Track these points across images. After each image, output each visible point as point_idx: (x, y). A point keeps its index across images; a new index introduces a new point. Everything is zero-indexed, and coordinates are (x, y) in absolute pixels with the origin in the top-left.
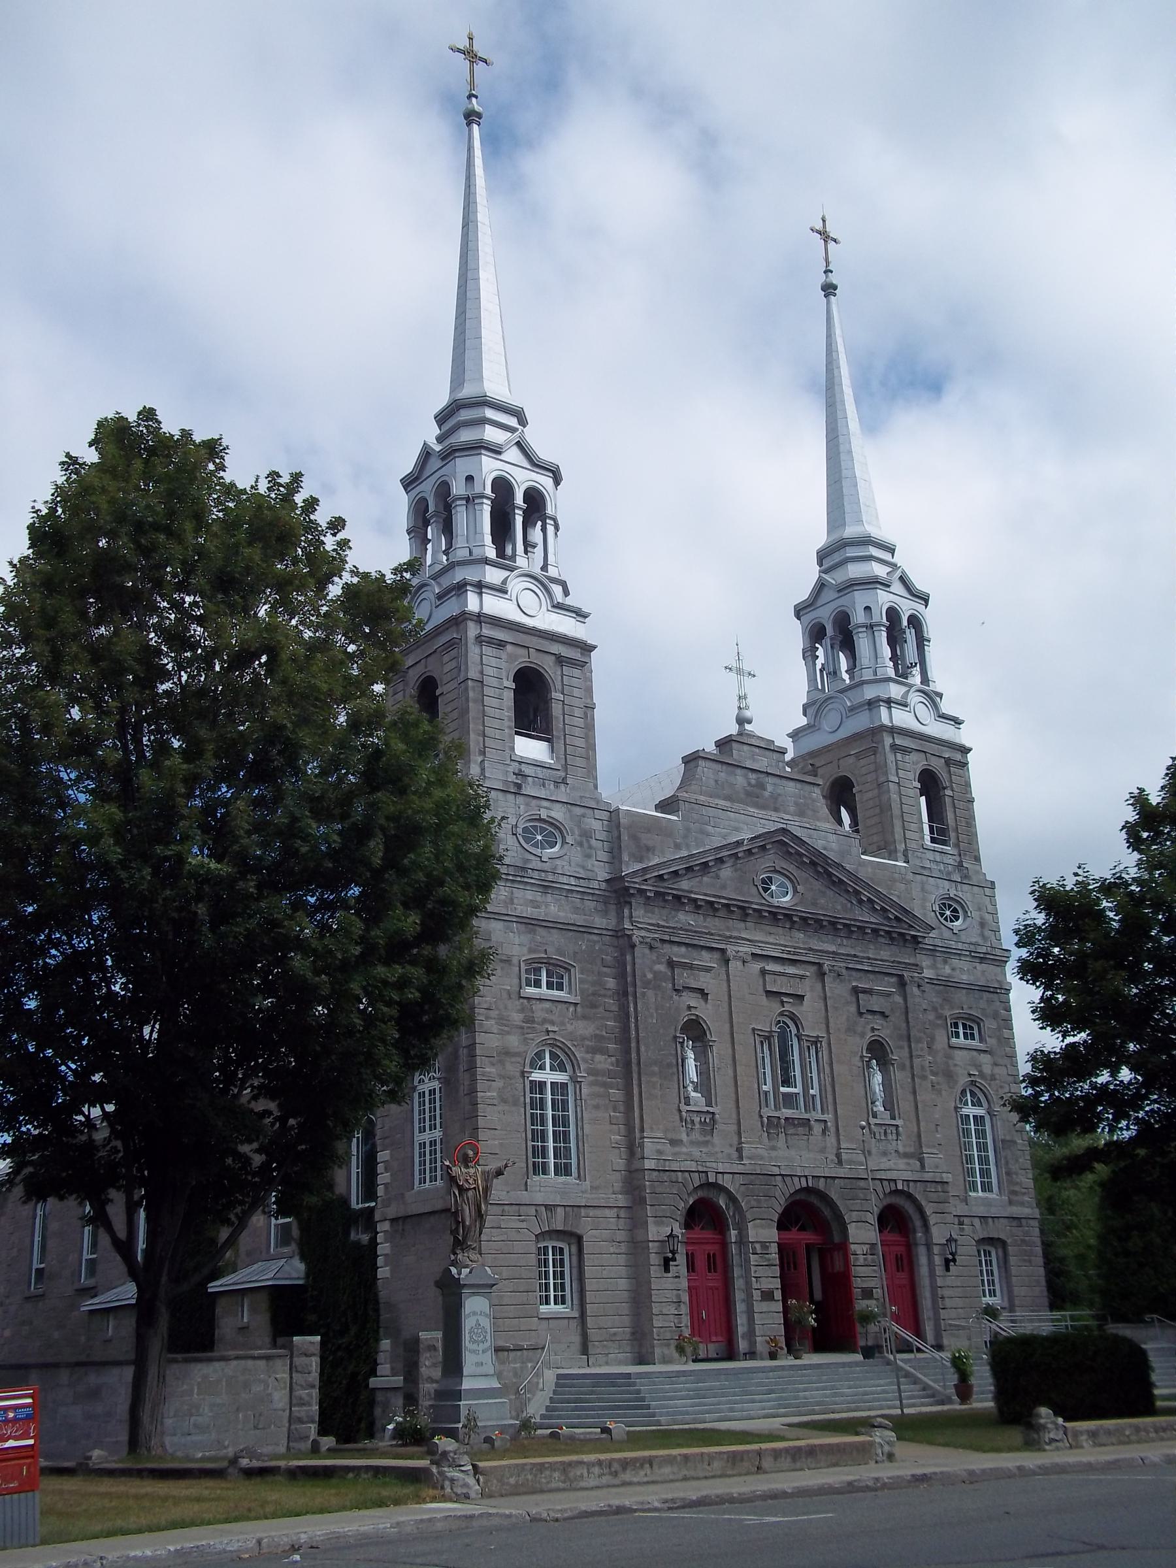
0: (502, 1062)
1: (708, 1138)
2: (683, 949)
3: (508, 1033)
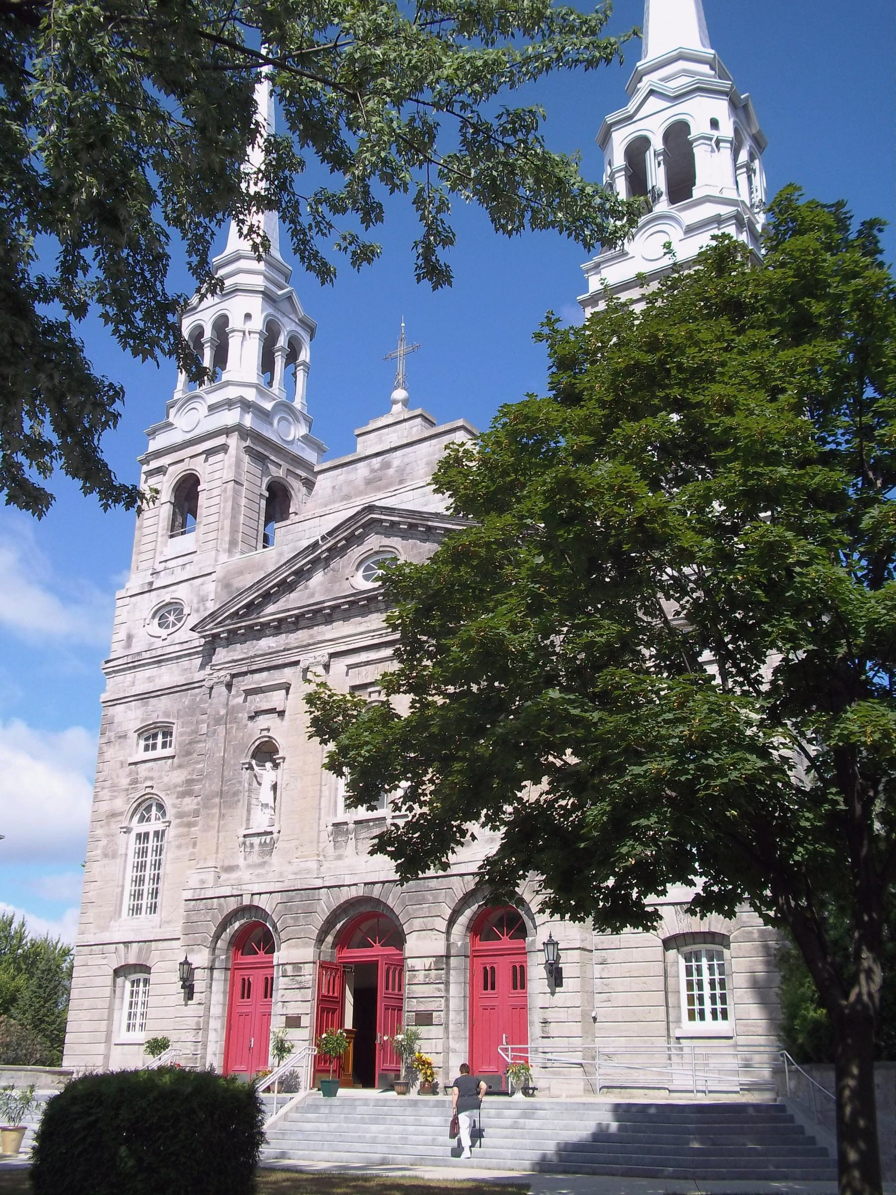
0: (108, 824)
1: (267, 858)
2: (265, 674)
3: (116, 797)
